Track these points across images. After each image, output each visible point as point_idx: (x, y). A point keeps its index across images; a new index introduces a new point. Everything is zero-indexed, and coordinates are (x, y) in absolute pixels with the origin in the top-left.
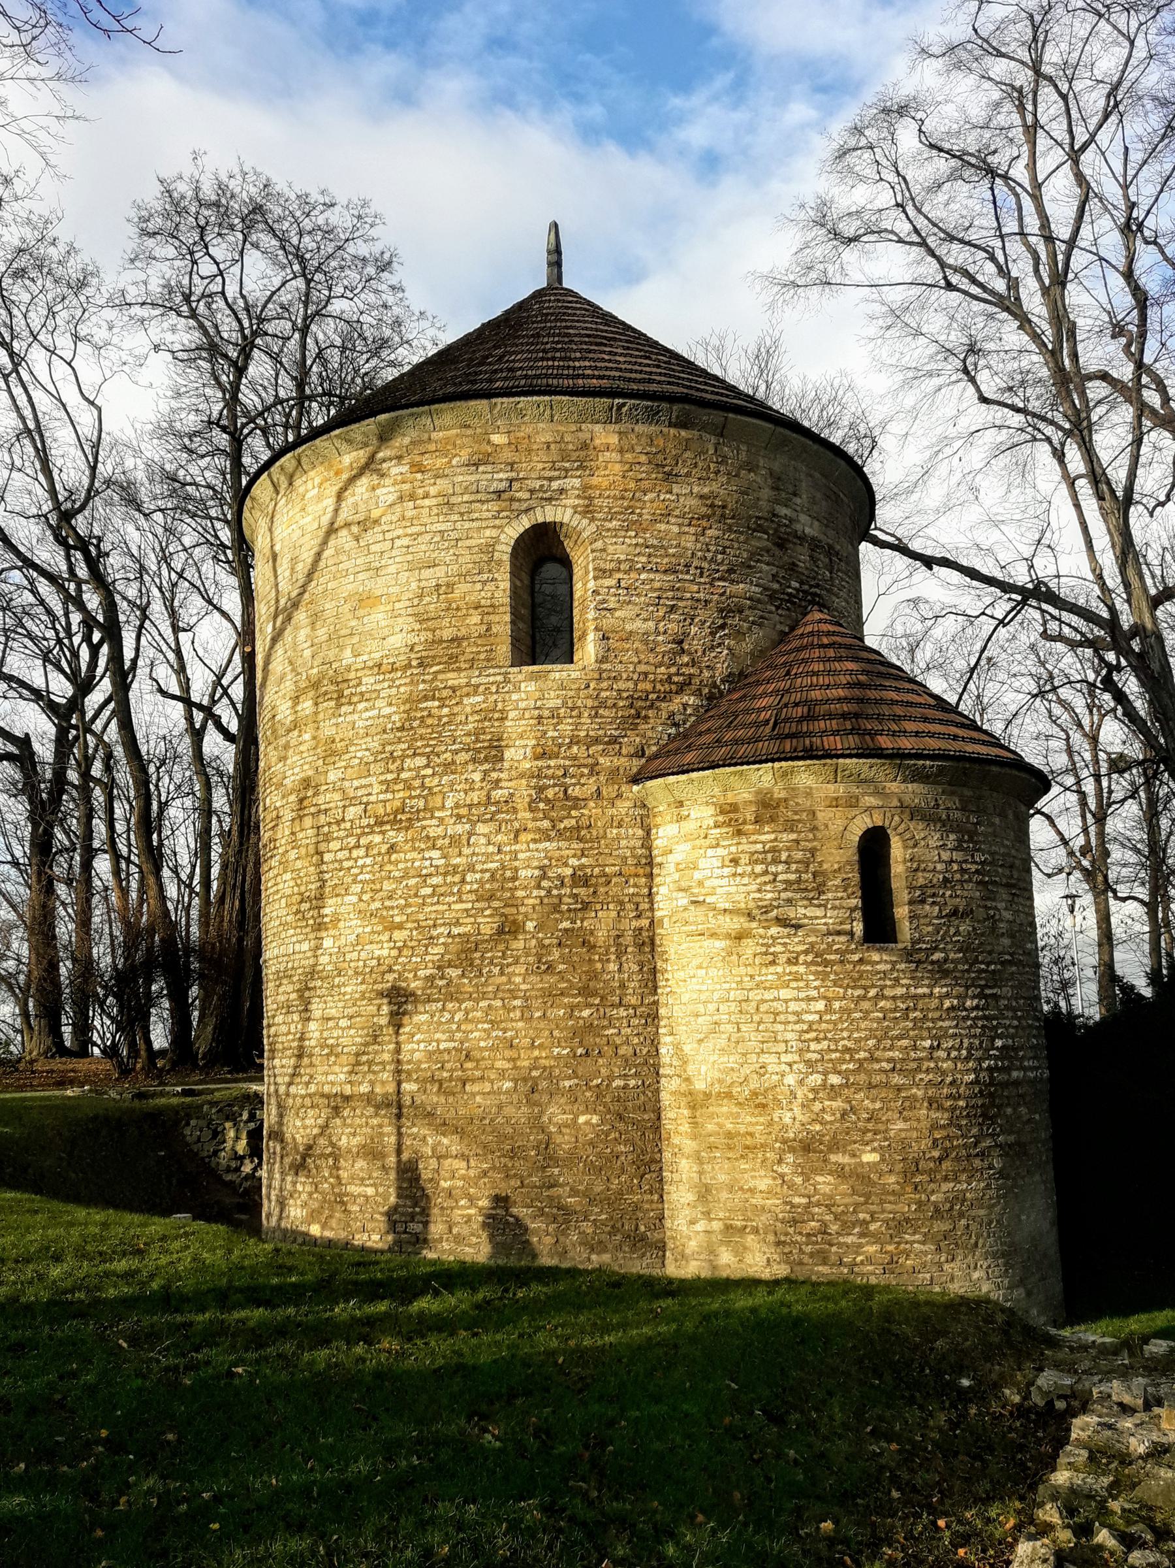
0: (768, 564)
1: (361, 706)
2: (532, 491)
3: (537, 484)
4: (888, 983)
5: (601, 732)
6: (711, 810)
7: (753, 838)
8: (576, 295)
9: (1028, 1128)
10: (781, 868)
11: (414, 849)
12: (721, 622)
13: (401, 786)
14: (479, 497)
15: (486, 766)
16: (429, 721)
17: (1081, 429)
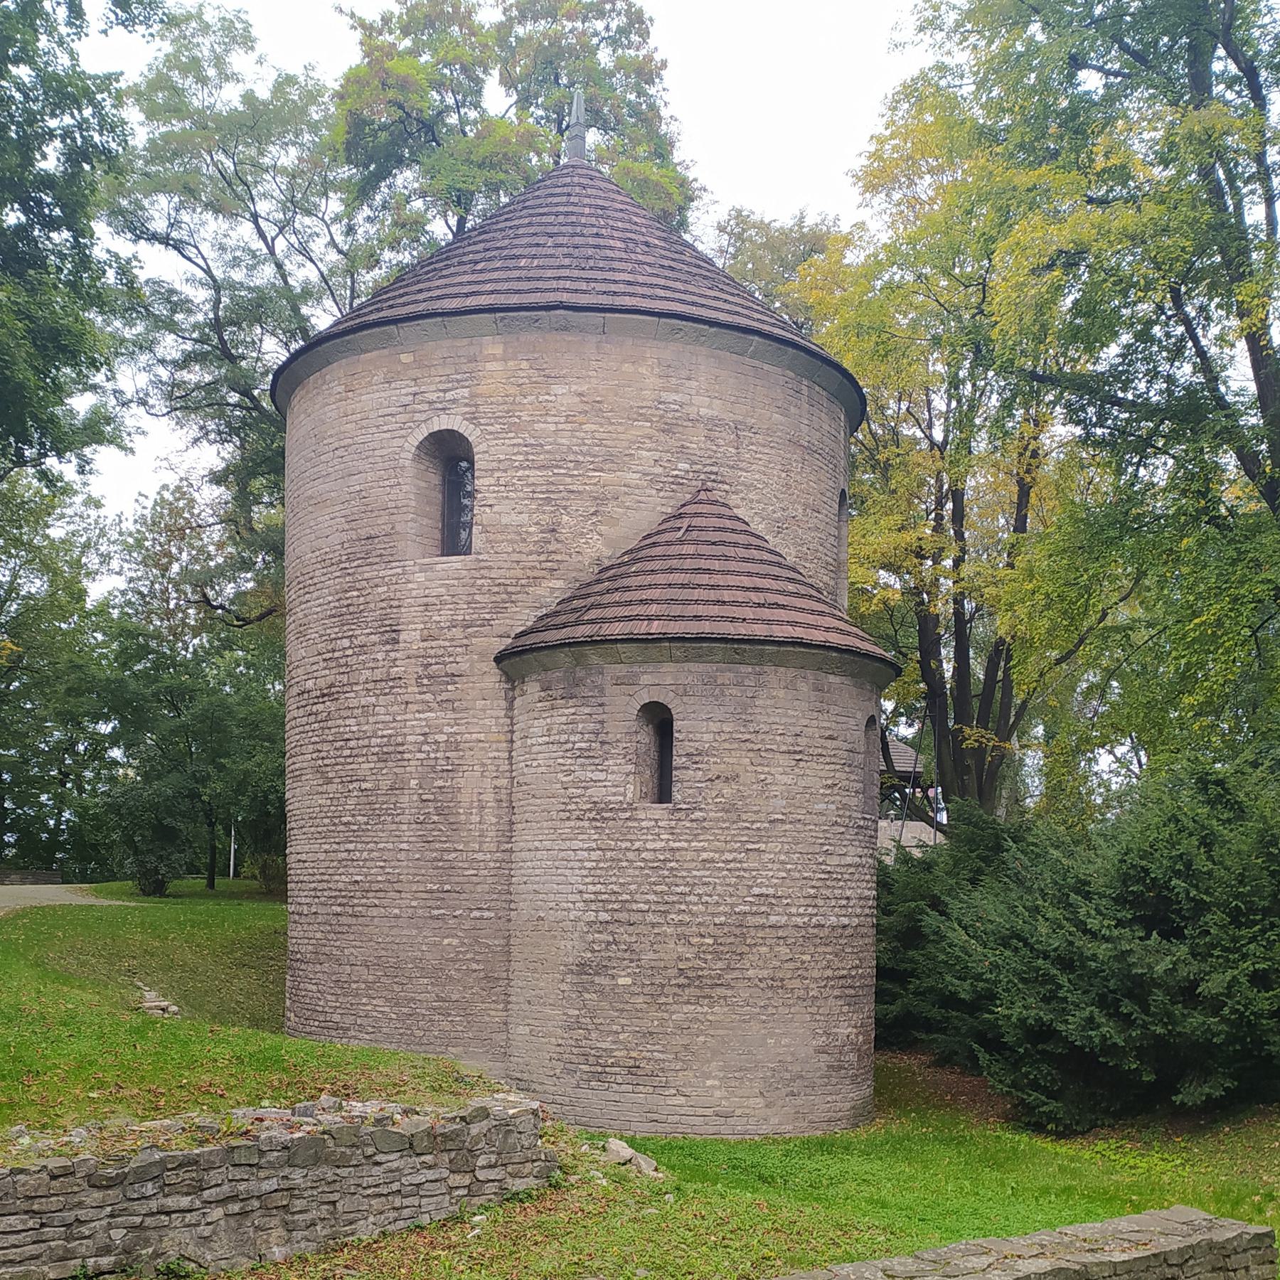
0: (649, 450)
1: (315, 595)
3: (433, 397)
4: (650, 837)
6: (537, 686)
9: (791, 965)
10: (578, 737)
12: (593, 510)
13: (334, 664)
15: (388, 647)
16: (351, 609)
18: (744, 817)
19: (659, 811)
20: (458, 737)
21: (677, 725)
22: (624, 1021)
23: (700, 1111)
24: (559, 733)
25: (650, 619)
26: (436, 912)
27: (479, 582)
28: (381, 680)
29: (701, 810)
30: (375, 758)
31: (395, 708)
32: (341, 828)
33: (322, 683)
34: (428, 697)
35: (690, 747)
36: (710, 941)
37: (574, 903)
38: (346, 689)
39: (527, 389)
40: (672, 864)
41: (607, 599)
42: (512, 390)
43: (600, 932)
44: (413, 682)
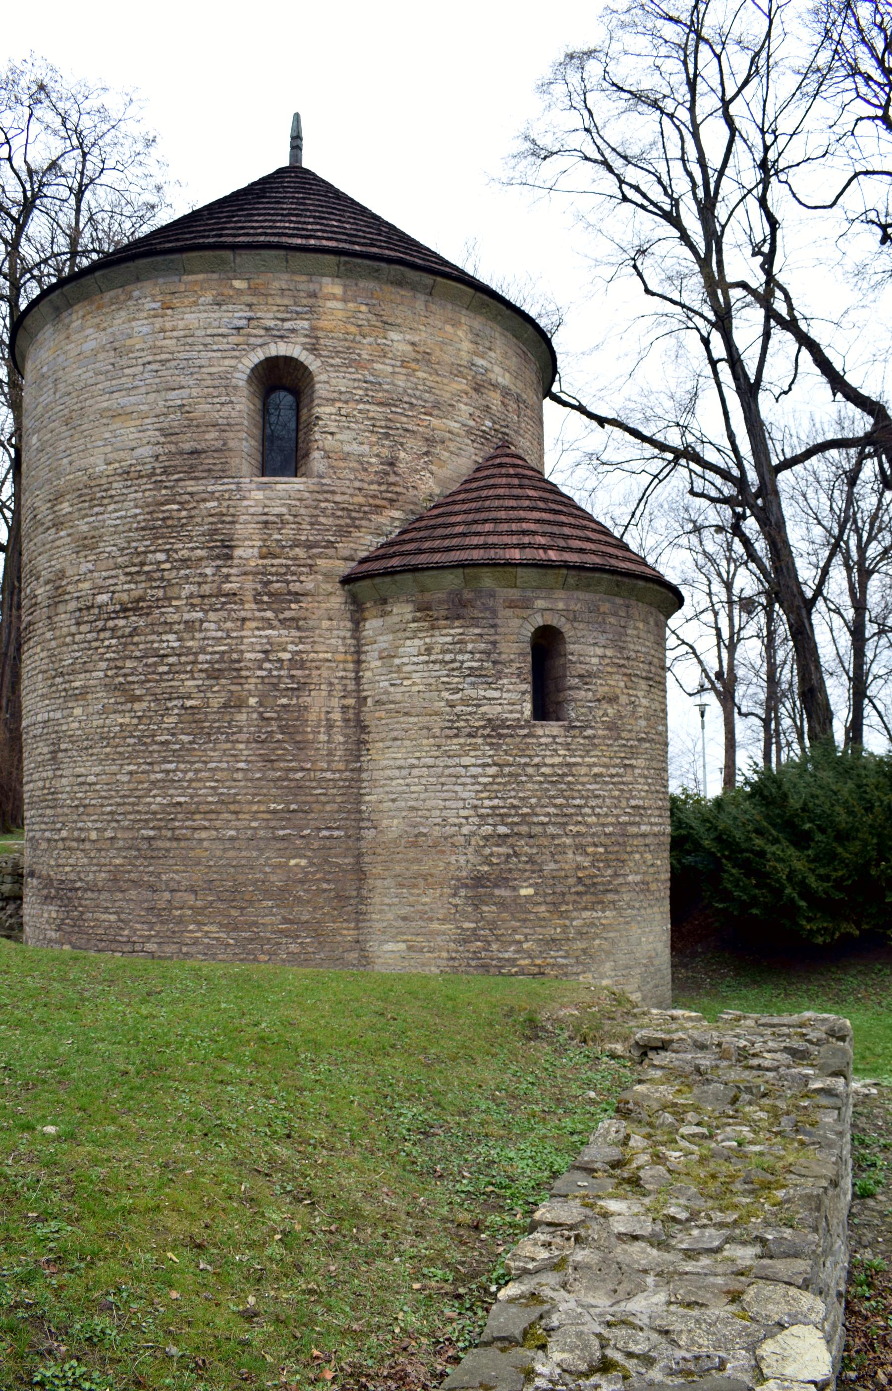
1: (111, 508)
2: (267, 329)
3: (271, 324)
5: (319, 538)
6: (409, 608)
7: (444, 632)
8: (313, 174)
9: (651, 870)
10: (467, 656)
11: (154, 633)
13: (143, 578)
14: (220, 331)
15: (219, 562)
16: (169, 522)
17: (723, 322)
18: (624, 734)
19: (553, 728)
21: (571, 647)
24: (444, 652)
25: (544, 548)
26: (281, 833)
27: (323, 505)
28: (210, 596)
29: (592, 728)
30: (203, 675)
31: (229, 625)
32: (156, 747)
33: (125, 597)
34: (269, 614)
35: (580, 669)
36: (601, 850)
37: (466, 818)
38: (160, 603)
39: (366, 330)
40: (570, 779)
41: (479, 528)
42: (353, 329)
43: (499, 845)
44: (251, 598)
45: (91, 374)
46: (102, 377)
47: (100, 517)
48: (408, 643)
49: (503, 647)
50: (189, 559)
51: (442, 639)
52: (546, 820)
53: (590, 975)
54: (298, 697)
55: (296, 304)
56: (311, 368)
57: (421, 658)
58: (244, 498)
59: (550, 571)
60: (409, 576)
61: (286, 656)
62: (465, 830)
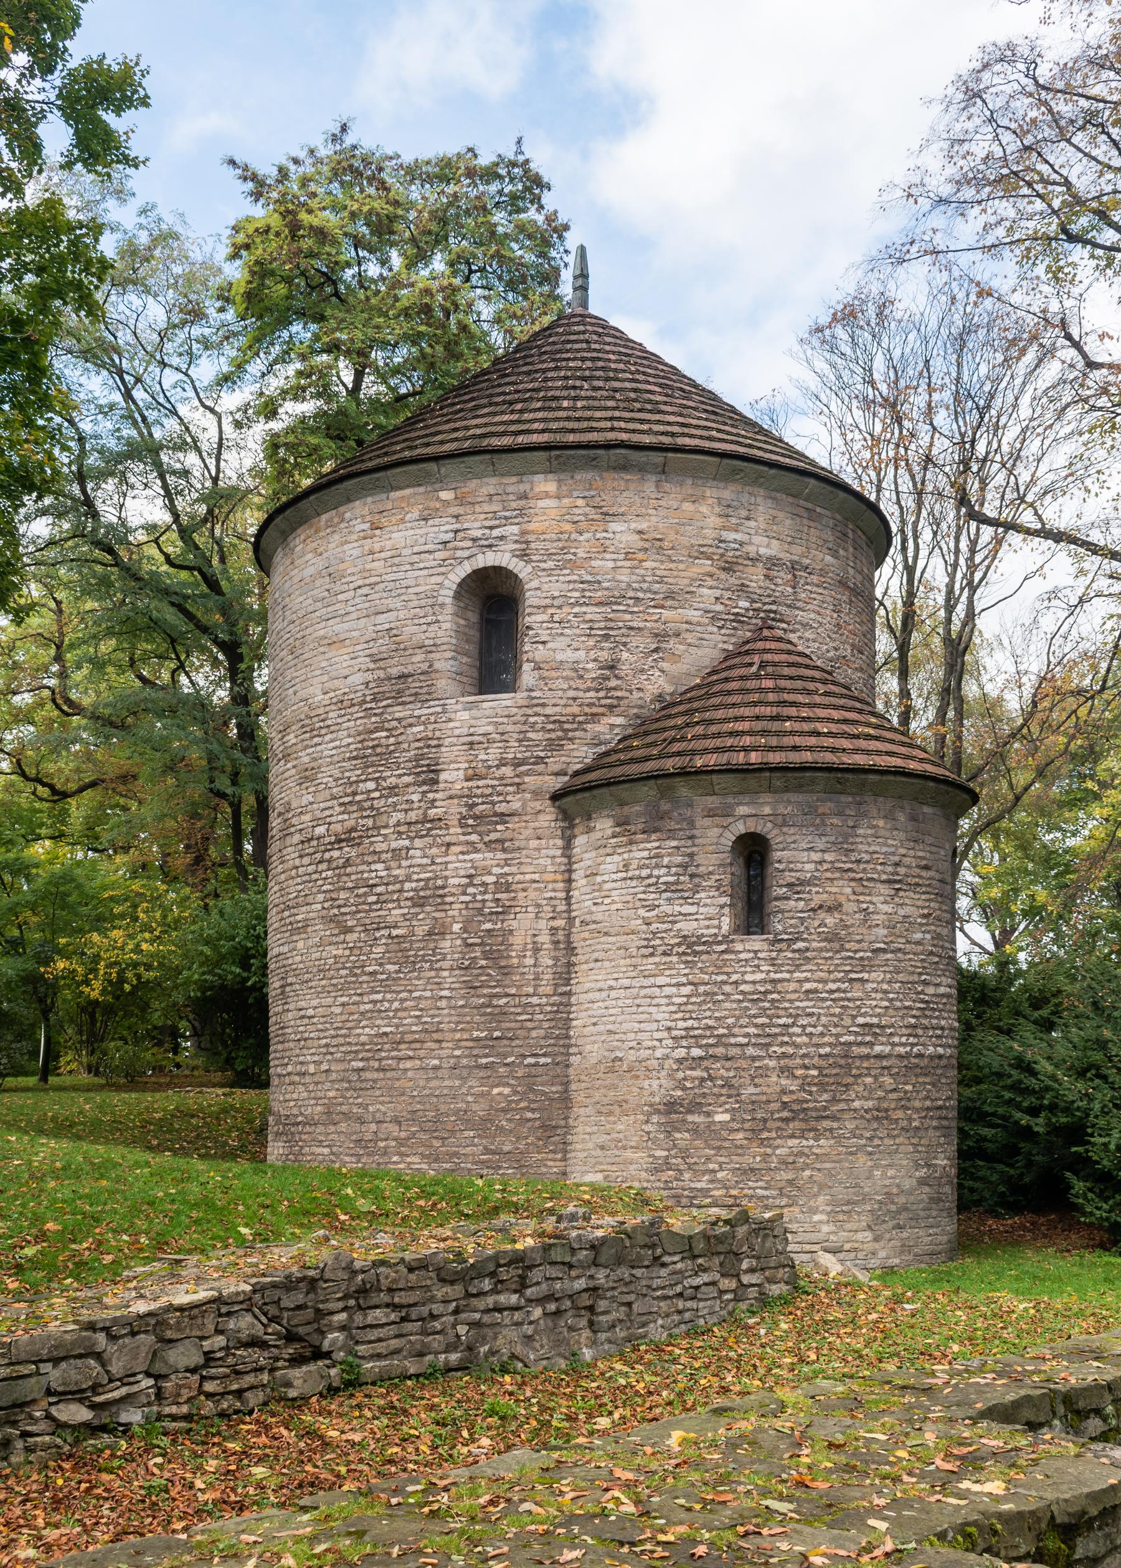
2: (474, 540)
3: (478, 533)
5: (528, 754)
6: (609, 823)
7: (642, 846)
10: (663, 871)
13: (355, 808)
14: (426, 548)
15: (425, 788)
16: (379, 750)
19: (756, 942)
20: (510, 879)
22: (723, 1159)
23: (807, 1247)
24: (640, 868)
25: (745, 749)
27: (532, 720)
28: (416, 822)
30: (409, 903)
31: (434, 851)
33: (338, 828)
34: (474, 838)
37: (660, 1040)
40: (775, 996)
44: (456, 823)
45: (310, 601)
46: (319, 604)
47: (319, 748)
48: (609, 859)
49: (700, 859)
50: (396, 787)
51: (639, 854)
52: (745, 1040)
53: (796, 1209)
54: (503, 921)
55: (505, 509)
56: (521, 576)
57: (620, 875)
58: (450, 720)
59: (749, 776)
60: (604, 790)
61: (490, 879)
62: (659, 1053)
